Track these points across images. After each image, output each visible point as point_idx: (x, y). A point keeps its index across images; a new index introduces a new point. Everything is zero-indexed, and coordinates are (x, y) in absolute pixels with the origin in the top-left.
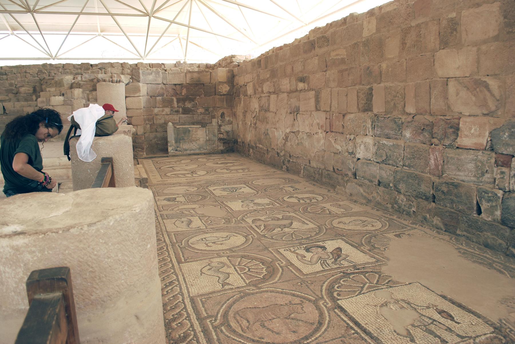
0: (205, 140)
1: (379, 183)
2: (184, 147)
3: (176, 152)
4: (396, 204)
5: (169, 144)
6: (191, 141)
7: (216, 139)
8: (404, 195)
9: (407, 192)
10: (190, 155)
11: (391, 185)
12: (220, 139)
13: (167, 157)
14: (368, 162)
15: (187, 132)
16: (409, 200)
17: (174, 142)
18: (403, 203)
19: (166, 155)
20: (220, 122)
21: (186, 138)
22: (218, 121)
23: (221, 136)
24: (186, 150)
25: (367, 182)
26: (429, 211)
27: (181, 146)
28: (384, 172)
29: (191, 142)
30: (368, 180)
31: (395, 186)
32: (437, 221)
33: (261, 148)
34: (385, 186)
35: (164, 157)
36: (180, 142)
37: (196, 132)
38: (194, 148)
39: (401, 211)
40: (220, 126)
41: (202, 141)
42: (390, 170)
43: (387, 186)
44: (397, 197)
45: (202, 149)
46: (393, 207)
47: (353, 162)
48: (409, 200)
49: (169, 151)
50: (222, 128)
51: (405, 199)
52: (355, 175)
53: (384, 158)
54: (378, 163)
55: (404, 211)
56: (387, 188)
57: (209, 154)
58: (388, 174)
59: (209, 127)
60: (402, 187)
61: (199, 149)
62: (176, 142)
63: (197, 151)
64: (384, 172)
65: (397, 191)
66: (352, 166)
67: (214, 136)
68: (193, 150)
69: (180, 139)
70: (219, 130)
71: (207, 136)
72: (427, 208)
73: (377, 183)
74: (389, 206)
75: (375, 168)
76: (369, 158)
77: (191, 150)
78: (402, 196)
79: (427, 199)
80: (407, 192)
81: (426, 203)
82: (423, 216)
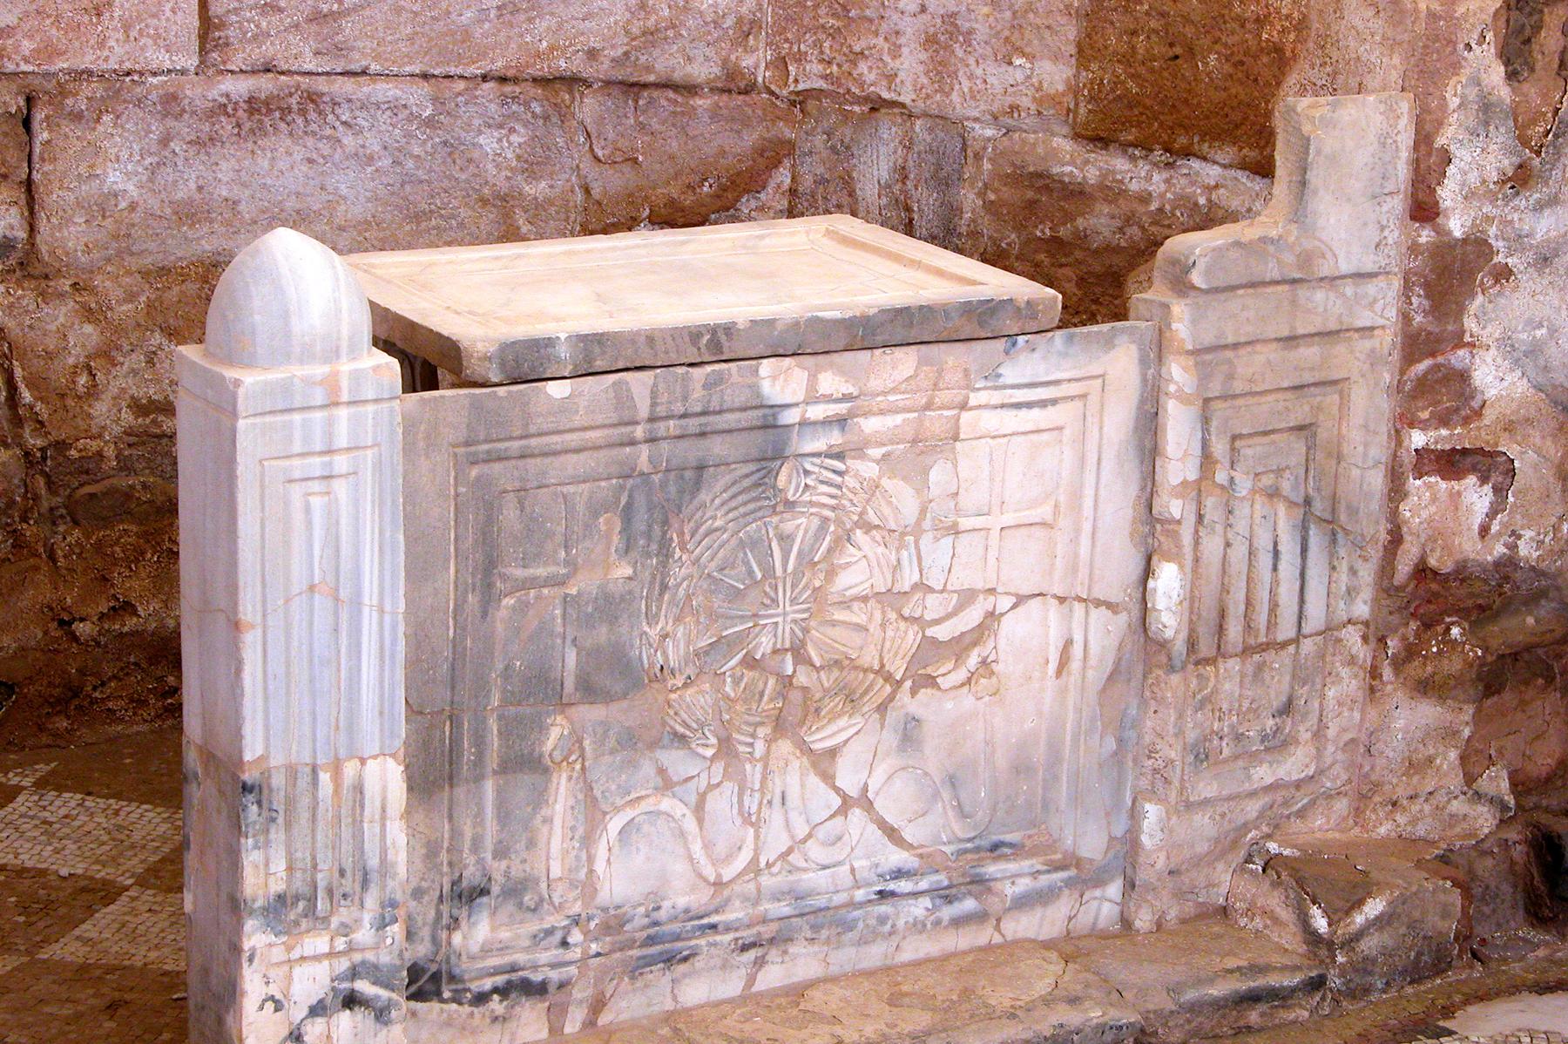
0: (1102, 635)
2: (622, 878)
5: (264, 869)
6: (792, 703)
7: (1342, 593)
12: (1430, 601)
15: (705, 445)
17: (387, 779)
20: (1475, 161)
21: (667, 639)
22: (1428, 166)
23: (1460, 520)
24: (662, 946)
27: (555, 850)
29: (791, 717)
36: (525, 763)
37: (924, 448)
38: (847, 858)
40: (1450, 276)
41: (1040, 669)
45: (1013, 877)
50: (1486, 317)
59: (1242, 316)
61: (964, 880)
62: (435, 772)
67: (1321, 517)
68: (823, 920)
69: (540, 690)
70: (1431, 373)
71: (1152, 538)
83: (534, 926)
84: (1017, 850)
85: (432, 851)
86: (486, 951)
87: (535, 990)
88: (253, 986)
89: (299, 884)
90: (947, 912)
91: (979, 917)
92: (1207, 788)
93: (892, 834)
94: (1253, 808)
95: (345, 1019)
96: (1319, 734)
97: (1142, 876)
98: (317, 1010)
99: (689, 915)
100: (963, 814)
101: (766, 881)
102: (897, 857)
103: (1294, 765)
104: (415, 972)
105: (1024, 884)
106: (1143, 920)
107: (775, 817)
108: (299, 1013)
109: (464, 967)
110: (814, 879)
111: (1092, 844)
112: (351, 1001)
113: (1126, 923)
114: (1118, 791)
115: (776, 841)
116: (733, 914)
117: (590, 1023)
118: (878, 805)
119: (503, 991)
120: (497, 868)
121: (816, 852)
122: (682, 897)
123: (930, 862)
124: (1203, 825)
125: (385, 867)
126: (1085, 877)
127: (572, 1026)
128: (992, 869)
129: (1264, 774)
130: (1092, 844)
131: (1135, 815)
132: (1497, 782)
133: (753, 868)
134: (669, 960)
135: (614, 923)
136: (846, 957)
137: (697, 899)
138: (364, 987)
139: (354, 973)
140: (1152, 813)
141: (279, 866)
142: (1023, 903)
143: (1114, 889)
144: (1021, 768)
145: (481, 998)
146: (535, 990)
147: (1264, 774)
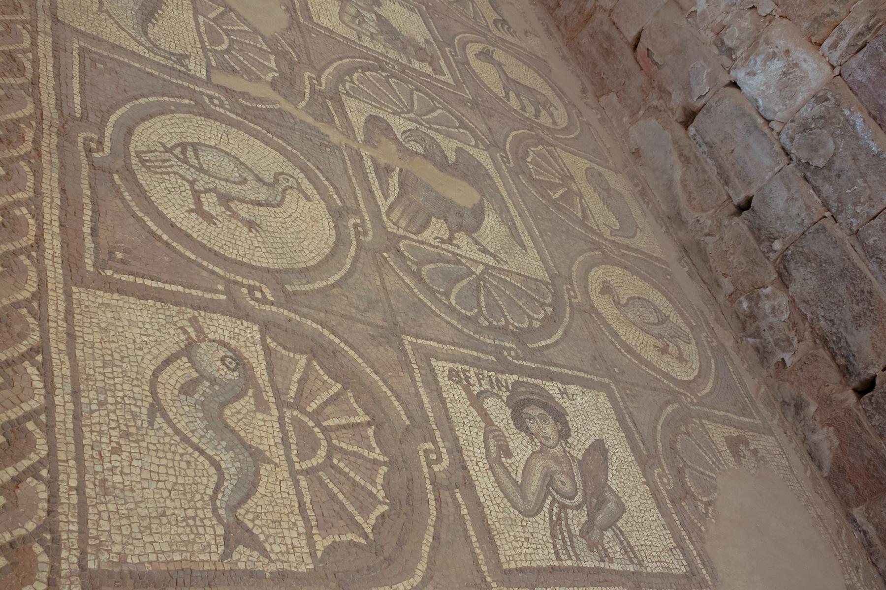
1: (745, 206)
4: (749, 298)
8: (792, 301)
9: (807, 302)
11: (777, 245)
14: (760, 121)
16: (795, 325)
18: (771, 319)
25: (711, 168)
26: (825, 402)
28: (784, 195)
30: (720, 167)
31: (784, 257)
32: (825, 440)
34: (756, 230)
39: (751, 329)
42: (808, 208)
43: (761, 234)
44: (768, 290)
46: (733, 297)
47: (713, 79)
48: (795, 325)
51: (785, 316)
52: (689, 117)
53: (819, 162)
54: (787, 154)
55: (757, 334)
56: (759, 240)
58: (794, 211)
60: (804, 280)
64: (784, 195)
65: (780, 275)
66: (702, 87)
72: (827, 390)
73: (739, 198)
74: (727, 286)
75: (767, 161)
76: (769, 116)
78: (782, 300)
79: (845, 371)
80: (807, 302)
81: (834, 375)
82: (799, 396)
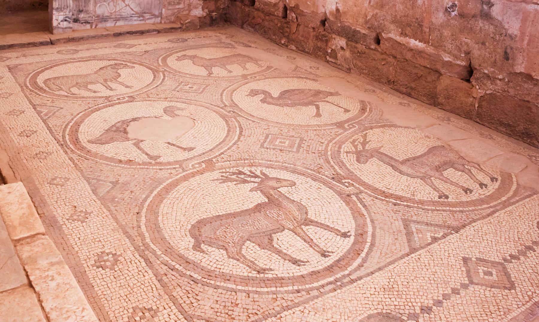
3: (76, 26)
10: (118, 35)
13: (52, 43)
19: (45, 37)
24: (103, 19)
33: (420, 53)
35: (42, 44)
38: (127, 12)
45: (147, 16)
49: (55, 23)
57: (172, 30)
61: (141, 15)
63: (136, 23)
68: (124, 18)
77: (117, 20)
83: (88, 15)
84: (147, 13)
85: (76, 6)
86: (83, 18)
87: (89, 23)
88: (54, 17)
89: (60, 6)
90: (139, 19)
91: (143, 20)
92: (170, 8)
93: (132, 9)
94: (176, 11)
95: (65, 23)
96: (184, 3)
97: (163, 17)
98: (62, 21)
99: (107, 16)
100: (141, 8)
101: (117, 13)
102: (133, 12)
103: (181, 6)
104: (74, 19)
105: (148, 17)
106: (163, 22)
107: (118, 6)
108: (60, 21)
109: (80, 19)
110: (123, 14)
111: (157, 13)
112: (66, 20)
113: (161, 23)
114: (160, 7)
115: (118, 9)
116: (113, 16)
117: (95, 27)
118: (131, 6)
119: (85, 23)
120: (84, 8)
121: (123, 10)
122: (106, 14)
123: (137, 13)
124: (170, 12)
125: (70, 6)
126: (156, 16)
127: (93, 27)
128: (145, 15)
129: (177, 7)
130: (157, 13)
131: (162, 10)
132: (206, 10)
133: (115, 12)
134: (105, 21)
135: (98, 16)
136: (127, 23)
137: (109, 15)
138: (67, 19)
139: (66, 17)
140: (164, 10)
141: (57, 4)
142: (148, 19)
143: (160, 19)
144: (148, 3)
145: (82, 23)
146: (89, 23)
147: (177, 7)
